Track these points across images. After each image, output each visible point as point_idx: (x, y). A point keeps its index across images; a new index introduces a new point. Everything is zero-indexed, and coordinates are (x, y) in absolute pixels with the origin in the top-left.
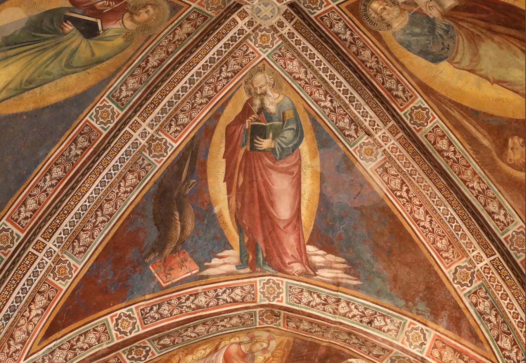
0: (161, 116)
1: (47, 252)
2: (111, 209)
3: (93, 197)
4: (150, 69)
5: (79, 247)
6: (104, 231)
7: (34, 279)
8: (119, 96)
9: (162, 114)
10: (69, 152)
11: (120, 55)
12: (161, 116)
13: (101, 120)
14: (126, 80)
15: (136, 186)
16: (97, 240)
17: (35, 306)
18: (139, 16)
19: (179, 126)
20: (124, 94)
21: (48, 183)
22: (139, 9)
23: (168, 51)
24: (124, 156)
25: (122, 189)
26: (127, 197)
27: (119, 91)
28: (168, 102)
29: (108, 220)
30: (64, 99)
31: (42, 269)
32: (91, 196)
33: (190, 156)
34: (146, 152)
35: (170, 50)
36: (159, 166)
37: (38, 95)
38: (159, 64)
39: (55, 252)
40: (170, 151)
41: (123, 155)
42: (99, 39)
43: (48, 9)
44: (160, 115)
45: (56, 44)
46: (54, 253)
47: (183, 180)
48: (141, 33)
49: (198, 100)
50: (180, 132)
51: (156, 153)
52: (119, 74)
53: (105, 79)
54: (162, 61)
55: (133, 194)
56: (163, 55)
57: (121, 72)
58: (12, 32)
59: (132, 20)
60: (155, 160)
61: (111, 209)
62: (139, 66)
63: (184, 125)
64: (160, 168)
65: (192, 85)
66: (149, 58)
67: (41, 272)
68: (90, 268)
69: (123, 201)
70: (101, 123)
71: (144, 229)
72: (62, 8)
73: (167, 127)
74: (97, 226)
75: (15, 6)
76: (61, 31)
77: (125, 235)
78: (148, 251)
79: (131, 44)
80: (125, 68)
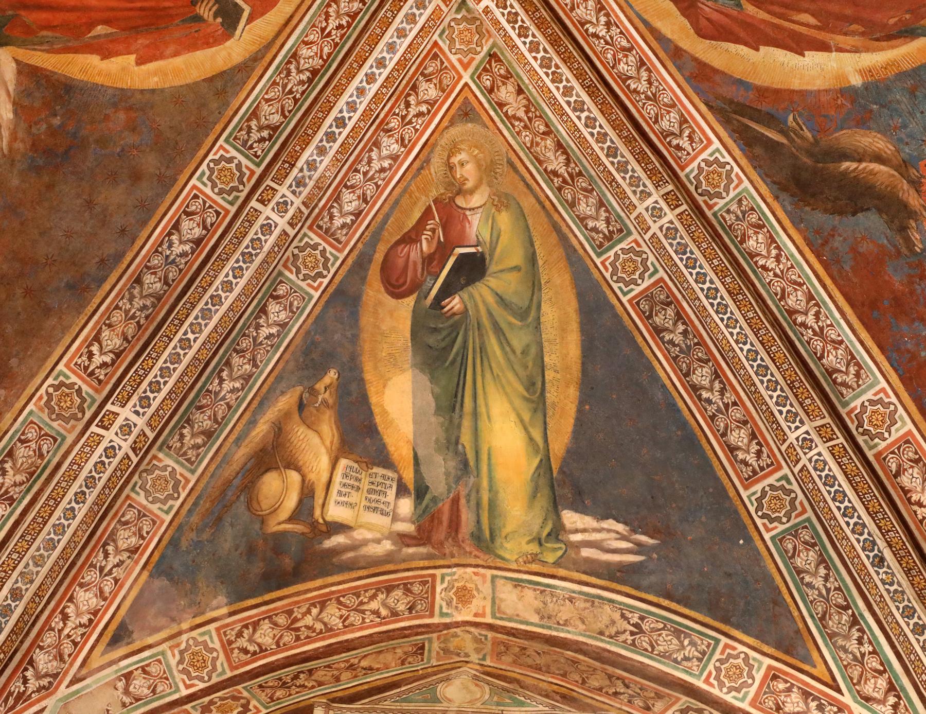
0: (630, 173)
1: (802, 448)
2: (799, 293)
3: (738, 333)
4: (570, 170)
5: (847, 373)
6: (834, 318)
7: (836, 487)
8: (604, 234)
9: (626, 172)
10: (674, 345)
11: (530, 222)
12: (630, 173)
13: (637, 277)
14: (578, 216)
15: (771, 236)
16: (847, 336)
17: (916, 492)
18: (467, 179)
19: (681, 131)
20: (602, 225)
21: (716, 397)
22: (454, 178)
23: (544, 133)
24: (684, 257)
25: (771, 264)
26: (788, 259)
27: (593, 234)
28: (607, 156)
29: (817, 305)
30: (579, 334)
31: (827, 467)
32: (735, 337)
33: (740, 118)
34: (716, 204)
35: (542, 128)
36: (746, 183)
37: (559, 376)
38: (565, 152)
39: (807, 433)
40: (724, 157)
41: (681, 259)
42: (491, 255)
43: (408, 335)
44: (628, 176)
45: (479, 329)
46: (809, 434)
47: (785, 141)
48: (499, 178)
49: (642, 86)
50: (694, 131)
51: (723, 185)
52: (564, 229)
53: (567, 254)
54: (559, 146)
55: (785, 245)
56: (548, 142)
57: (562, 224)
58: (430, 398)
59: (472, 192)
60: (735, 189)
61: (799, 293)
62: (560, 189)
63: (683, 121)
64: (751, 182)
65: (586, 107)
66: (549, 169)
67: (830, 470)
68: (892, 366)
69: (792, 267)
70: (642, 277)
71: (856, 239)
72: (414, 311)
73: (680, 154)
74: (821, 329)
75: (384, 387)
76: (457, 317)
77: (855, 280)
78: (899, 240)
79: (515, 199)
80: (556, 217)
